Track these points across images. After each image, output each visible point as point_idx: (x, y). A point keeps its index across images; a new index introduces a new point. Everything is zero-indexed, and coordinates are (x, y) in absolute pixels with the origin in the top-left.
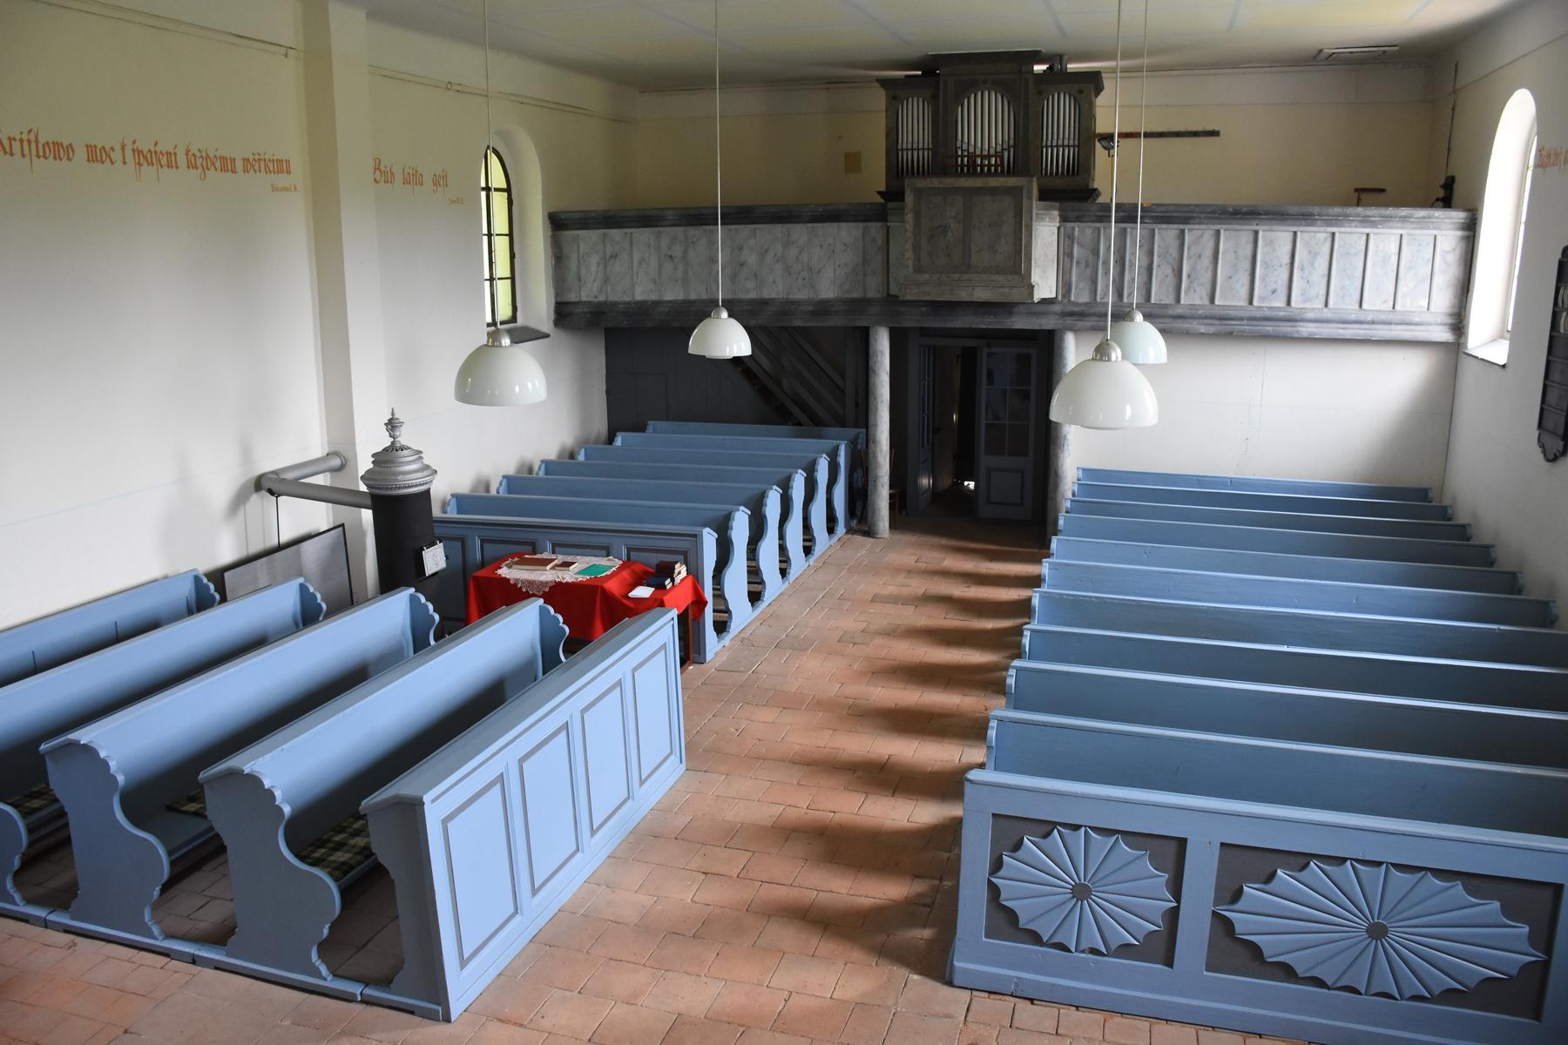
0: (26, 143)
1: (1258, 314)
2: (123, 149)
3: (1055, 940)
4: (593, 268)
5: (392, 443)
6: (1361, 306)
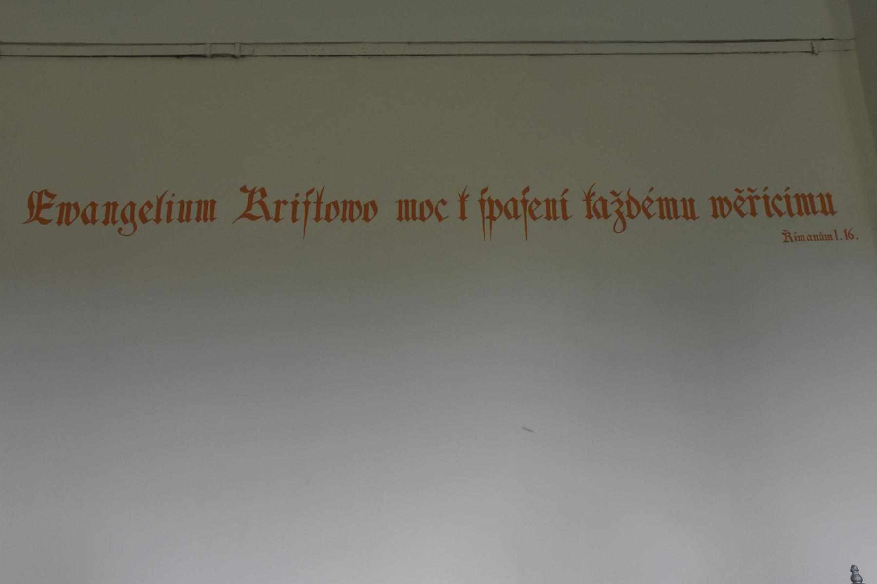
0: (301, 208)
2: (463, 200)
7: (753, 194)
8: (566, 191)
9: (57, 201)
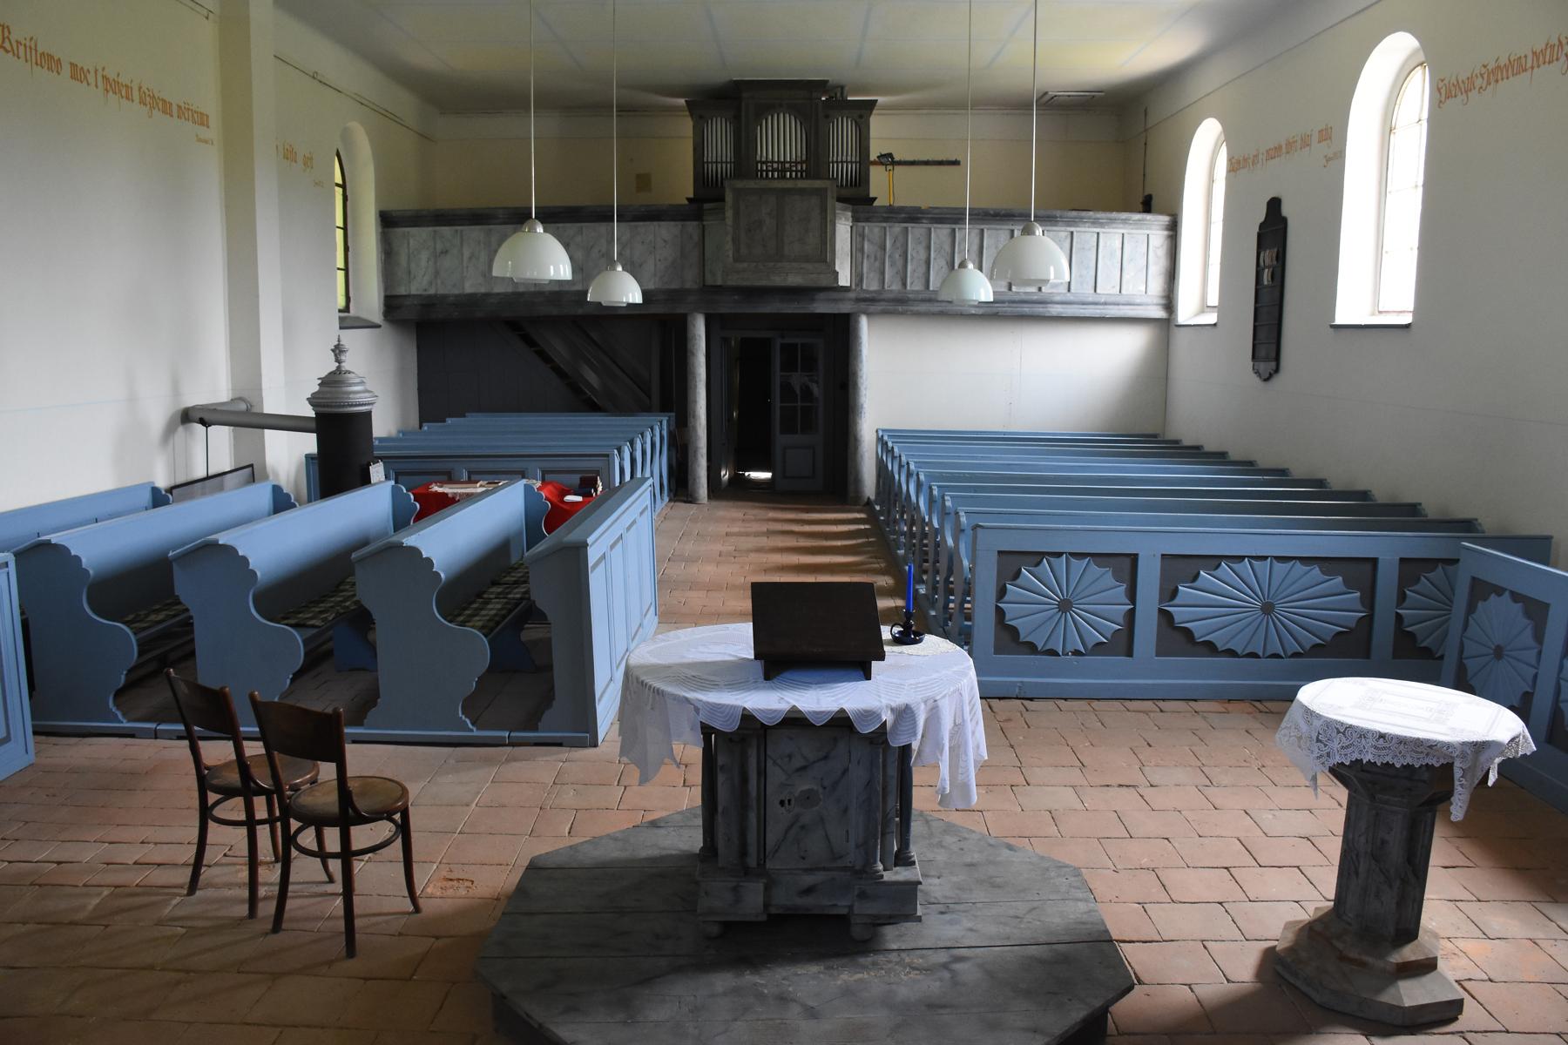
0: (28, 50)
1: (1017, 298)
3: (1047, 647)
4: (423, 263)
5: (339, 368)
6: (1095, 291)
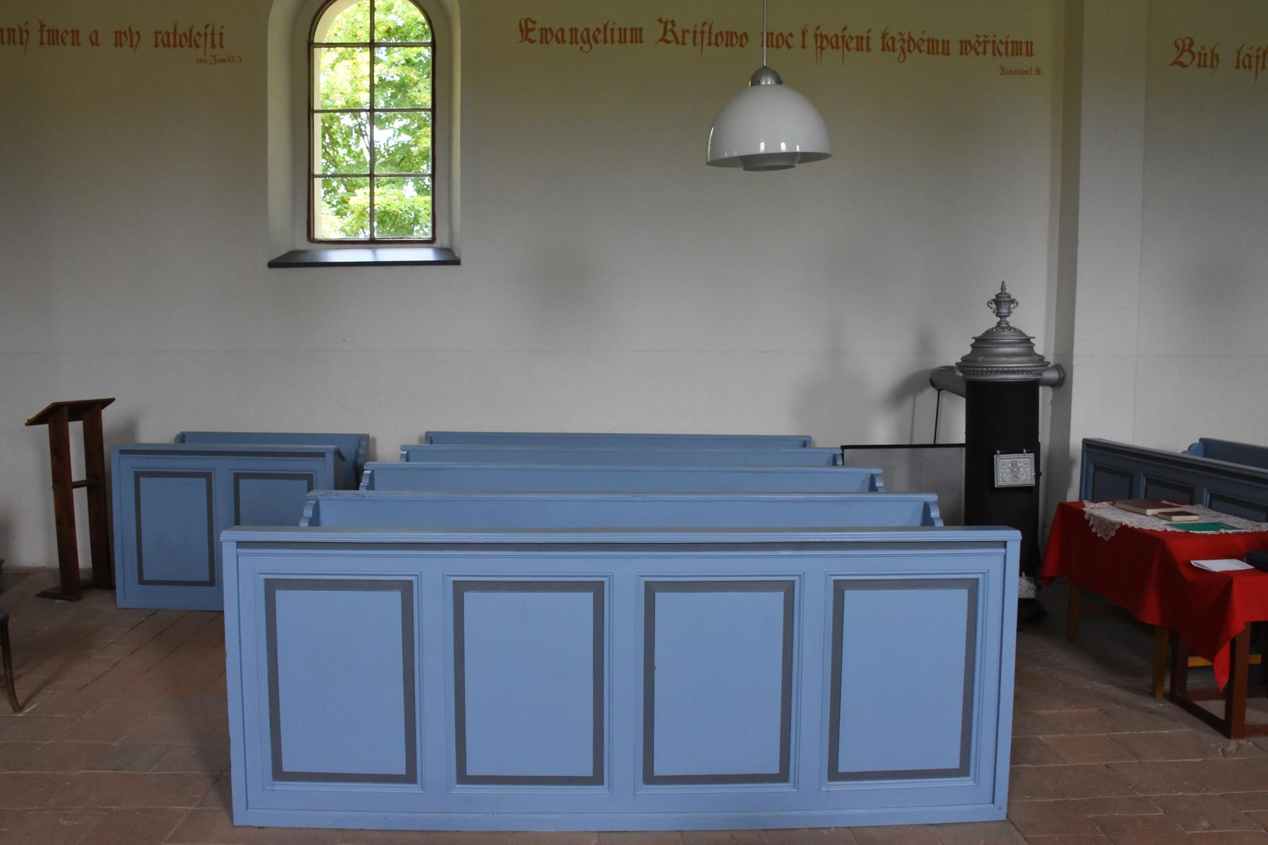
0: (699, 35)
2: (804, 33)
7: (987, 39)
8: (870, 30)
9: (538, 26)
